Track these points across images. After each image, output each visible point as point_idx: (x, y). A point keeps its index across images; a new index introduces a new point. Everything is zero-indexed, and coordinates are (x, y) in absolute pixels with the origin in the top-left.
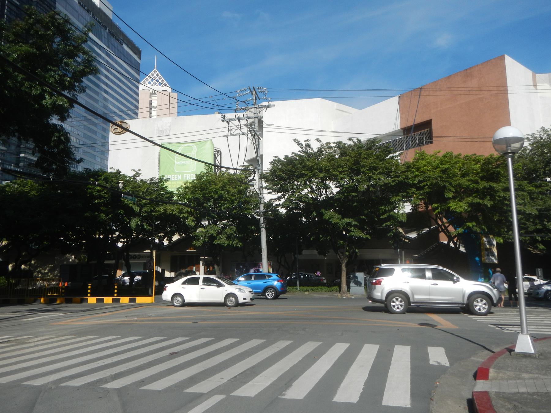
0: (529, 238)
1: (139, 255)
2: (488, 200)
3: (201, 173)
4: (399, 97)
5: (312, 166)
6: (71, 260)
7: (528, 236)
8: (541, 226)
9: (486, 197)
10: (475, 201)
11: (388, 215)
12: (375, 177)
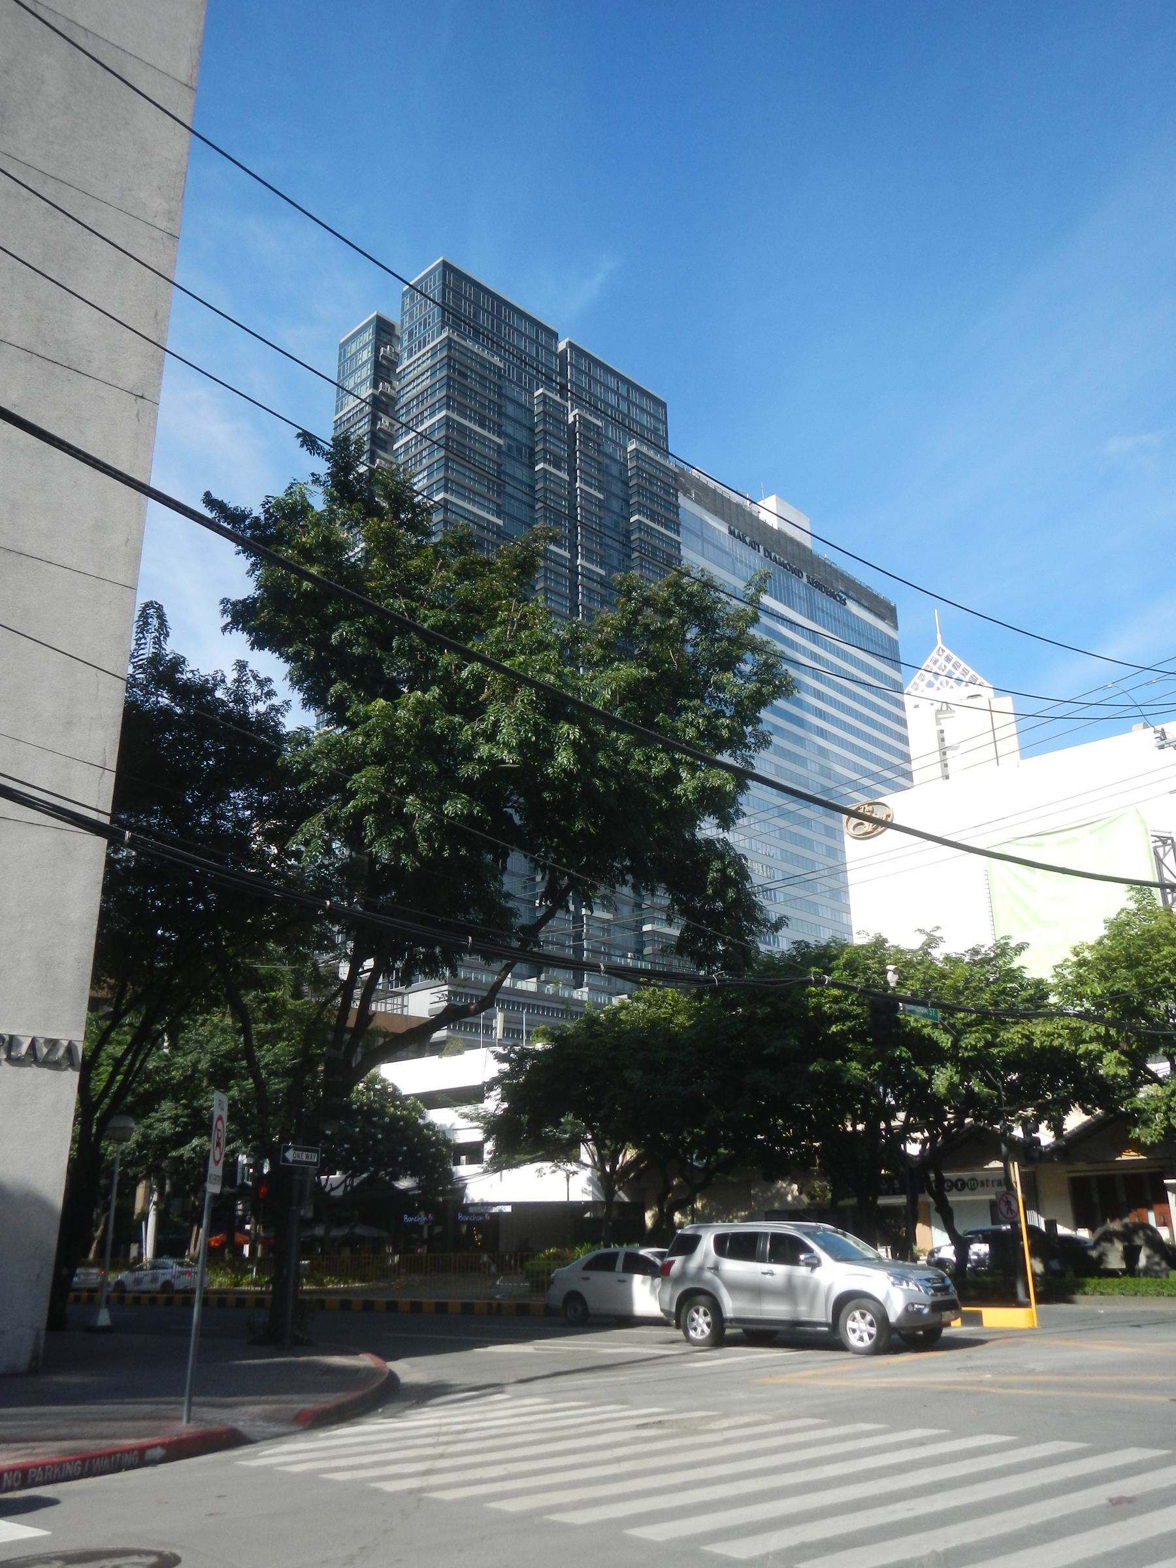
1: (972, 1179)
3: (1119, 913)
6: (789, 1198)
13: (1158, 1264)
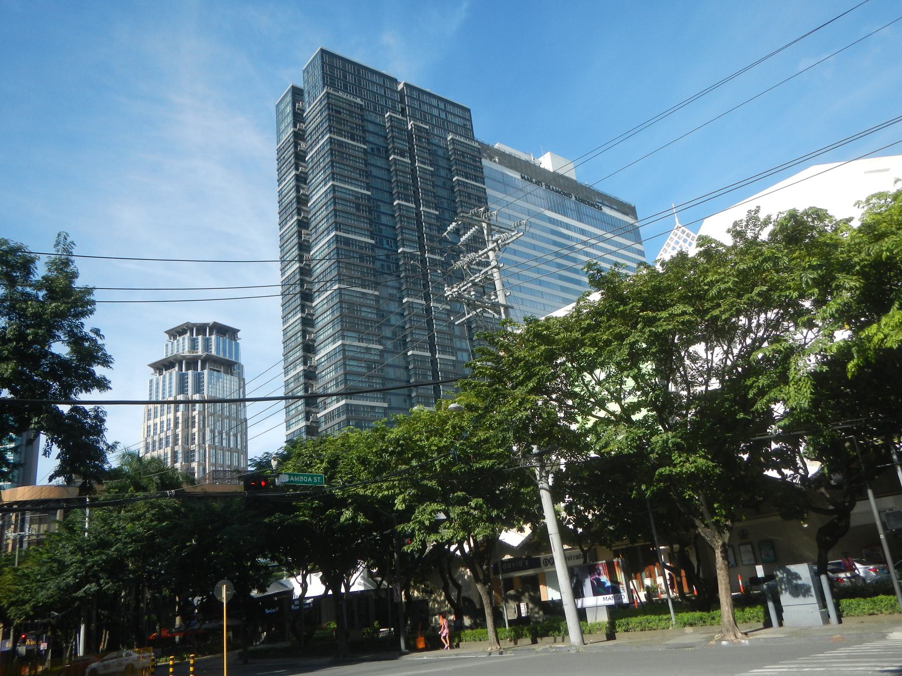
6: (466, 577)
13: (538, 613)
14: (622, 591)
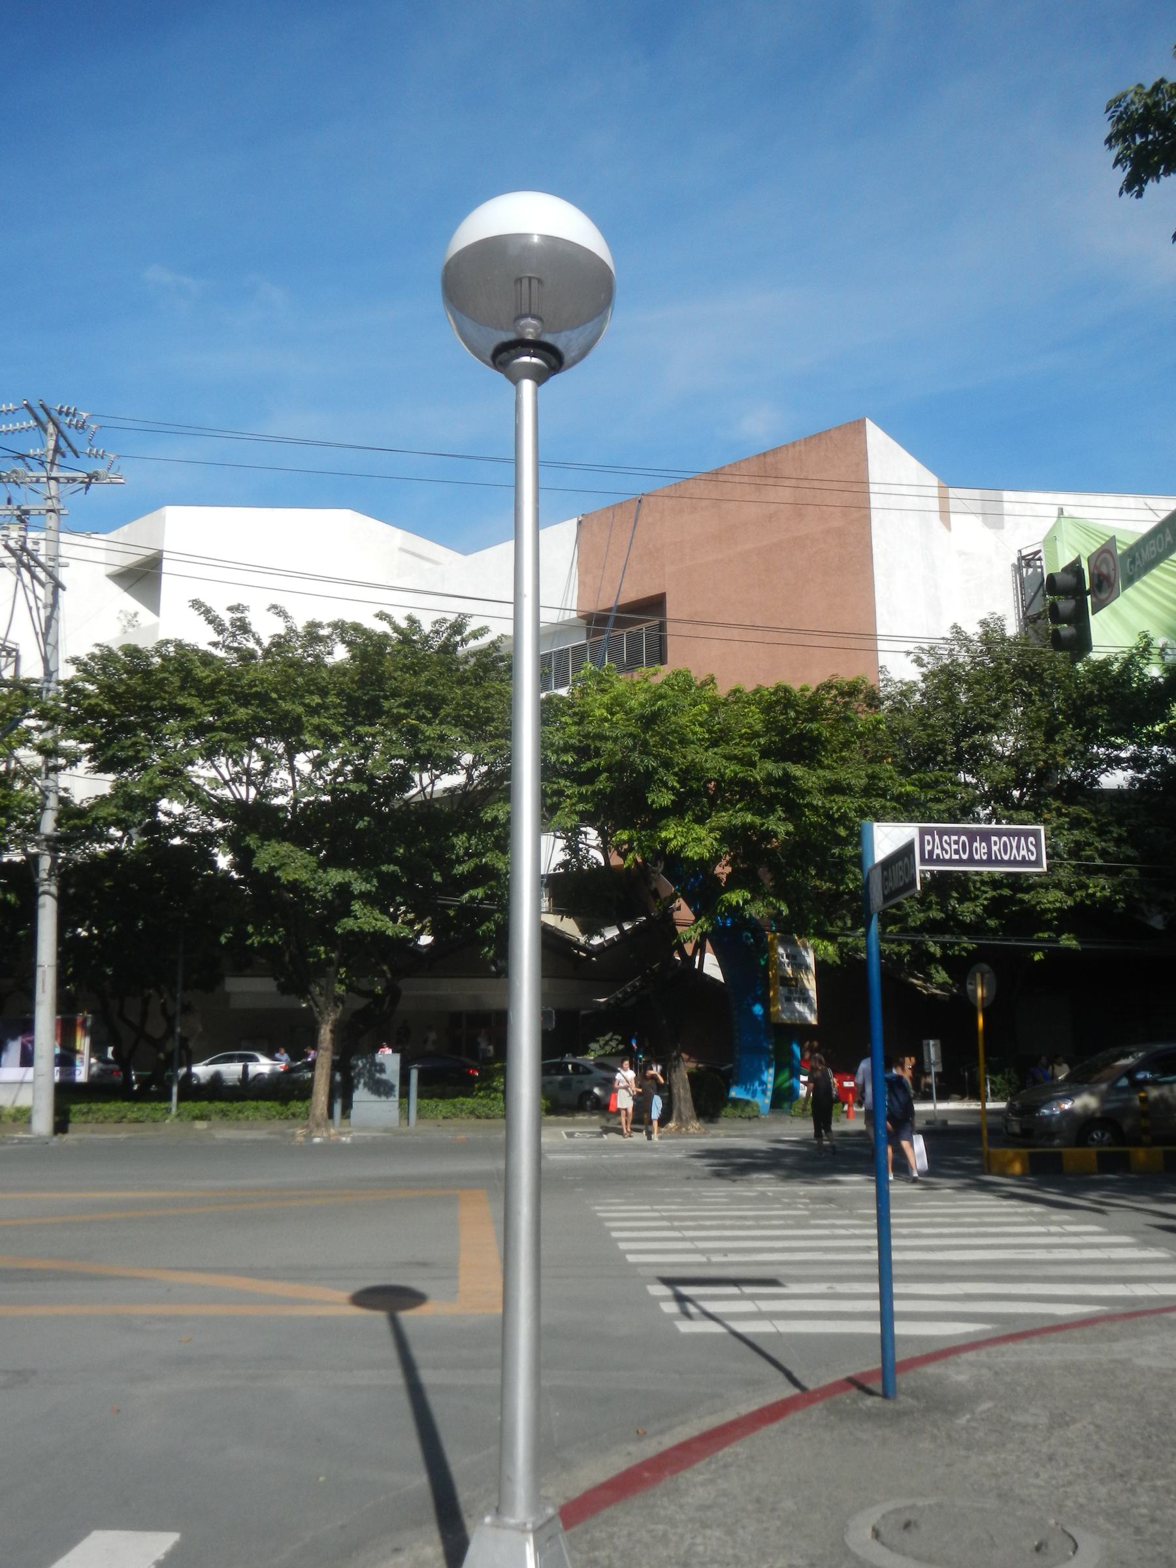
0: (908, 947)
2: (779, 819)
4: (580, 523)
5: (218, 682)
7: (909, 942)
8: (941, 911)
9: (773, 811)
10: (737, 821)
11: (476, 865)
12: (429, 731)
14: (78, 1063)
